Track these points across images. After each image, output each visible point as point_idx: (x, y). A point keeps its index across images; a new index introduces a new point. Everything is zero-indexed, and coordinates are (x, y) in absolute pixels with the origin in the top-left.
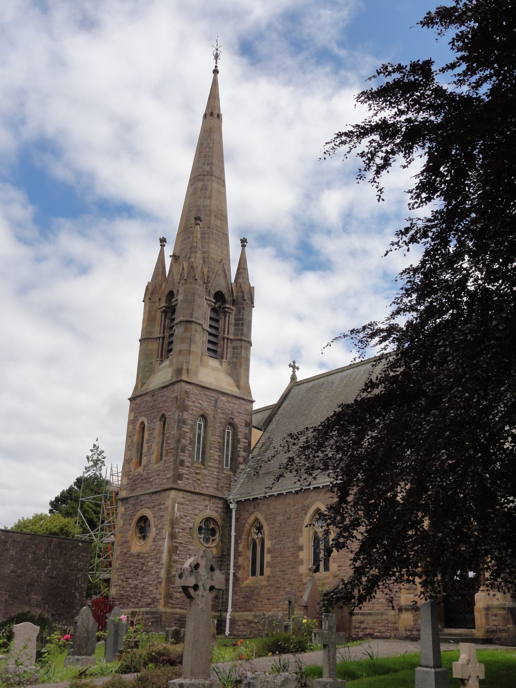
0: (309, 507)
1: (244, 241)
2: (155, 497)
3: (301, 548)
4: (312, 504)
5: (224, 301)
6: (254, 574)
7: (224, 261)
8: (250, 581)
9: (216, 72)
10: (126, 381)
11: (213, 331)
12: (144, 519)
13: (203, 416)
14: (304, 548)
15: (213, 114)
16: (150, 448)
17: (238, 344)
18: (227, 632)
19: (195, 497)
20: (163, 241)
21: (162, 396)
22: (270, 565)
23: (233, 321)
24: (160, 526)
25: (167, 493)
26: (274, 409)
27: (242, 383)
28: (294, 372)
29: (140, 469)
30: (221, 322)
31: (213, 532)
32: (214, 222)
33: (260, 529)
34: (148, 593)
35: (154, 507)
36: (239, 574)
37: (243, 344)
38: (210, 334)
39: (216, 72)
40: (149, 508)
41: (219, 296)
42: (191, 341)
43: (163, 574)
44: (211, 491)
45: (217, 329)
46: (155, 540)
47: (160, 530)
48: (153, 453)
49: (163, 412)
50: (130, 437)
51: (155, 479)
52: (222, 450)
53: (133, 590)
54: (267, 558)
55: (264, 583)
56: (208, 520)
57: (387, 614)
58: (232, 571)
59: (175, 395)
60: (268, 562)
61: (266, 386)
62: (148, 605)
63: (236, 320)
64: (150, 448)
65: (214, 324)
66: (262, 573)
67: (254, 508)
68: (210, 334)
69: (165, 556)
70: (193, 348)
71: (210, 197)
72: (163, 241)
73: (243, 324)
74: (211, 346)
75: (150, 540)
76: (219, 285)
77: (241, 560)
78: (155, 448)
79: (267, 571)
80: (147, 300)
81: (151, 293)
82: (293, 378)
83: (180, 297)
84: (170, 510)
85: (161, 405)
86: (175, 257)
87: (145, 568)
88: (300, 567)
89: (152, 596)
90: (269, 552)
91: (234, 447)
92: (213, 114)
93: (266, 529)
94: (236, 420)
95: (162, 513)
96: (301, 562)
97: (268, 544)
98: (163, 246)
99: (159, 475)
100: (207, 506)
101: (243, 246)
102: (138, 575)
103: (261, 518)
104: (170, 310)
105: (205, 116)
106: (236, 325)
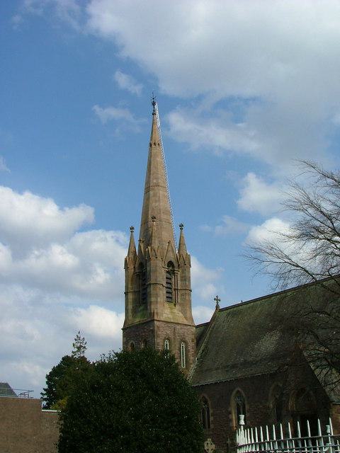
1: (181, 226)
5: (173, 266)
11: (169, 286)
20: (132, 228)
23: (179, 279)
27: (188, 315)
30: (173, 280)
32: (163, 217)
33: (206, 402)
37: (187, 292)
38: (167, 288)
41: (170, 264)
42: (157, 296)
45: (170, 284)
54: (211, 419)
61: (202, 314)
63: (182, 277)
65: (169, 281)
66: (209, 427)
68: (167, 288)
70: (159, 300)
71: (159, 200)
74: (168, 295)
76: (171, 257)
79: (212, 426)
82: (217, 307)
93: (209, 403)
94: (187, 339)
97: (211, 411)
106: (181, 280)
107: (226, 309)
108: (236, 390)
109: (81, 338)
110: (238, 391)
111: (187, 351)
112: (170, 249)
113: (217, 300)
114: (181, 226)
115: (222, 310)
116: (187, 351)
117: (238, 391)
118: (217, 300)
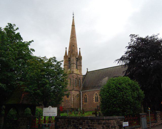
0: (95, 93)
1: (80, 48)
3: (94, 99)
7: (77, 53)
9: (73, 17)
13: (76, 79)
15: (73, 25)
17: (80, 66)
20: (66, 48)
22: (88, 101)
26: (85, 76)
27: (81, 73)
33: (86, 96)
36: (83, 102)
43: (72, 103)
46: (70, 98)
47: (71, 96)
54: (88, 100)
58: (81, 102)
61: (84, 73)
72: (66, 48)
73: (80, 63)
76: (77, 57)
77: (83, 100)
79: (88, 102)
82: (87, 71)
83: (72, 59)
86: (69, 52)
91: (80, 83)
92: (73, 25)
93: (87, 96)
96: (94, 101)
97: (88, 98)
98: (66, 49)
104: (69, 61)
105: (72, 26)
106: (80, 63)
107: (90, 72)
108: (96, 93)
111: (81, 82)
112: (77, 54)
113: (87, 69)
114: (80, 48)
115: (89, 72)
116: (81, 82)
118: (87, 69)
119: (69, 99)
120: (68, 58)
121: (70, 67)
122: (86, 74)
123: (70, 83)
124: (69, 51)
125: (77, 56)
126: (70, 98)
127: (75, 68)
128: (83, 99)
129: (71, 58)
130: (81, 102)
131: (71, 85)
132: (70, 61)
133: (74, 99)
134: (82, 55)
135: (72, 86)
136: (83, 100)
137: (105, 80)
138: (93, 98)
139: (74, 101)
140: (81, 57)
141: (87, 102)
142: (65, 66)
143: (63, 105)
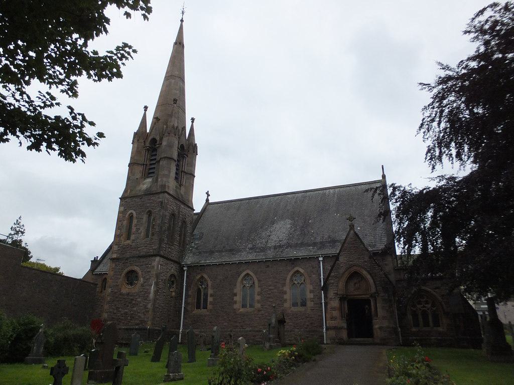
0: (241, 273)
1: (193, 120)
2: (142, 260)
3: (235, 295)
4: (244, 271)
6: (198, 307)
7: (184, 128)
8: (196, 311)
9: (182, 21)
10: (120, 186)
12: (132, 272)
14: (238, 294)
15: (179, 44)
16: (138, 229)
18: (325, 341)
19: (168, 262)
20: (146, 108)
21: (150, 200)
24: (148, 277)
25: (153, 258)
28: (208, 197)
29: (128, 242)
31: (173, 282)
34: (137, 317)
35: (142, 265)
36: (189, 308)
39: (182, 21)
40: (137, 266)
43: (150, 306)
44: (174, 259)
47: (147, 280)
48: (141, 233)
49: (150, 209)
50: (120, 221)
51: (143, 249)
52: (180, 236)
53: (124, 315)
54: (210, 299)
55: (208, 313)
56: (172, 276)
57: (294, 331)
58: (183, 305)
59: (161, 200)
60: (210, 302)
62: (137, 324)
64: (138, 229)
67: (201, 270)
69: (152, 295)
72: (146, 108)
75: (139, 285)
77: (190, 300)
78: (143, 230)
79: (209, 306)
80: (136, 141)
81: (140, 136)
82: (207, 200)
83: (164, 143)
84: (156, 268)
85: (148, 205)
86: (156, 119)
87: (134, 302)
88: (234, 305)
89: (140, 319)
90: (211, 295)
92: (179, 44)
93: (210, 283)
95: (149, 270)
96: (236, 302)
97: (210, 291)
99: (146, 246)
100: (172, 268)
101: (193, 122)
102: (128, 306)
103: (206, 276)
105: (176, 43)
108: (244, 273)
109: (21, 224)
110: (248, 275)
114: (193, 120)
117: (248, 275)
119: (135, 289)
120: (150, 139)
121: (151, 171)
122: (204, 210)
123: (148, 227)
124: (157, 115)
125: (182, 137)
126: (142, 285)
127: (173, 174)
128: (190, 293)
129: (161, 139)
130: (183, 305)
131: (153, 234)
132: (155, 150)
133: (156, 292)
134: (197, 140)
135: (156, 237)
136: (190, 300)
137: (281, 231)
138: (235, 291)
139: (155, 300)
140: (195, 147)
141: (205, 307)
142: (135, 166)
143: (105, 315)
